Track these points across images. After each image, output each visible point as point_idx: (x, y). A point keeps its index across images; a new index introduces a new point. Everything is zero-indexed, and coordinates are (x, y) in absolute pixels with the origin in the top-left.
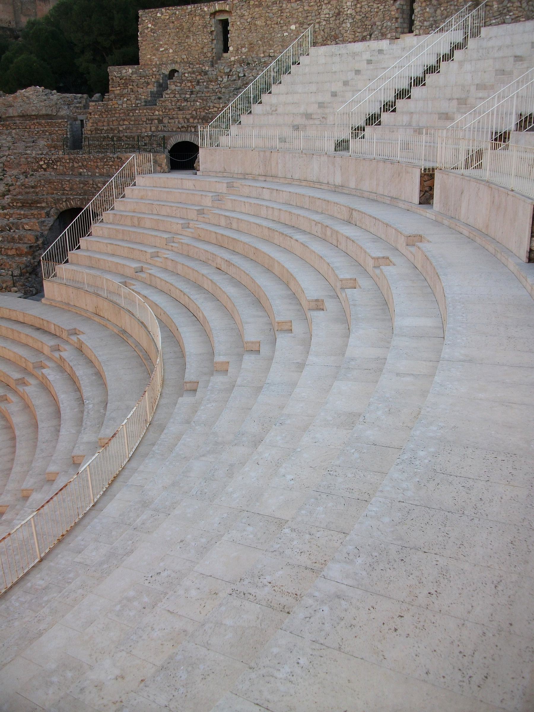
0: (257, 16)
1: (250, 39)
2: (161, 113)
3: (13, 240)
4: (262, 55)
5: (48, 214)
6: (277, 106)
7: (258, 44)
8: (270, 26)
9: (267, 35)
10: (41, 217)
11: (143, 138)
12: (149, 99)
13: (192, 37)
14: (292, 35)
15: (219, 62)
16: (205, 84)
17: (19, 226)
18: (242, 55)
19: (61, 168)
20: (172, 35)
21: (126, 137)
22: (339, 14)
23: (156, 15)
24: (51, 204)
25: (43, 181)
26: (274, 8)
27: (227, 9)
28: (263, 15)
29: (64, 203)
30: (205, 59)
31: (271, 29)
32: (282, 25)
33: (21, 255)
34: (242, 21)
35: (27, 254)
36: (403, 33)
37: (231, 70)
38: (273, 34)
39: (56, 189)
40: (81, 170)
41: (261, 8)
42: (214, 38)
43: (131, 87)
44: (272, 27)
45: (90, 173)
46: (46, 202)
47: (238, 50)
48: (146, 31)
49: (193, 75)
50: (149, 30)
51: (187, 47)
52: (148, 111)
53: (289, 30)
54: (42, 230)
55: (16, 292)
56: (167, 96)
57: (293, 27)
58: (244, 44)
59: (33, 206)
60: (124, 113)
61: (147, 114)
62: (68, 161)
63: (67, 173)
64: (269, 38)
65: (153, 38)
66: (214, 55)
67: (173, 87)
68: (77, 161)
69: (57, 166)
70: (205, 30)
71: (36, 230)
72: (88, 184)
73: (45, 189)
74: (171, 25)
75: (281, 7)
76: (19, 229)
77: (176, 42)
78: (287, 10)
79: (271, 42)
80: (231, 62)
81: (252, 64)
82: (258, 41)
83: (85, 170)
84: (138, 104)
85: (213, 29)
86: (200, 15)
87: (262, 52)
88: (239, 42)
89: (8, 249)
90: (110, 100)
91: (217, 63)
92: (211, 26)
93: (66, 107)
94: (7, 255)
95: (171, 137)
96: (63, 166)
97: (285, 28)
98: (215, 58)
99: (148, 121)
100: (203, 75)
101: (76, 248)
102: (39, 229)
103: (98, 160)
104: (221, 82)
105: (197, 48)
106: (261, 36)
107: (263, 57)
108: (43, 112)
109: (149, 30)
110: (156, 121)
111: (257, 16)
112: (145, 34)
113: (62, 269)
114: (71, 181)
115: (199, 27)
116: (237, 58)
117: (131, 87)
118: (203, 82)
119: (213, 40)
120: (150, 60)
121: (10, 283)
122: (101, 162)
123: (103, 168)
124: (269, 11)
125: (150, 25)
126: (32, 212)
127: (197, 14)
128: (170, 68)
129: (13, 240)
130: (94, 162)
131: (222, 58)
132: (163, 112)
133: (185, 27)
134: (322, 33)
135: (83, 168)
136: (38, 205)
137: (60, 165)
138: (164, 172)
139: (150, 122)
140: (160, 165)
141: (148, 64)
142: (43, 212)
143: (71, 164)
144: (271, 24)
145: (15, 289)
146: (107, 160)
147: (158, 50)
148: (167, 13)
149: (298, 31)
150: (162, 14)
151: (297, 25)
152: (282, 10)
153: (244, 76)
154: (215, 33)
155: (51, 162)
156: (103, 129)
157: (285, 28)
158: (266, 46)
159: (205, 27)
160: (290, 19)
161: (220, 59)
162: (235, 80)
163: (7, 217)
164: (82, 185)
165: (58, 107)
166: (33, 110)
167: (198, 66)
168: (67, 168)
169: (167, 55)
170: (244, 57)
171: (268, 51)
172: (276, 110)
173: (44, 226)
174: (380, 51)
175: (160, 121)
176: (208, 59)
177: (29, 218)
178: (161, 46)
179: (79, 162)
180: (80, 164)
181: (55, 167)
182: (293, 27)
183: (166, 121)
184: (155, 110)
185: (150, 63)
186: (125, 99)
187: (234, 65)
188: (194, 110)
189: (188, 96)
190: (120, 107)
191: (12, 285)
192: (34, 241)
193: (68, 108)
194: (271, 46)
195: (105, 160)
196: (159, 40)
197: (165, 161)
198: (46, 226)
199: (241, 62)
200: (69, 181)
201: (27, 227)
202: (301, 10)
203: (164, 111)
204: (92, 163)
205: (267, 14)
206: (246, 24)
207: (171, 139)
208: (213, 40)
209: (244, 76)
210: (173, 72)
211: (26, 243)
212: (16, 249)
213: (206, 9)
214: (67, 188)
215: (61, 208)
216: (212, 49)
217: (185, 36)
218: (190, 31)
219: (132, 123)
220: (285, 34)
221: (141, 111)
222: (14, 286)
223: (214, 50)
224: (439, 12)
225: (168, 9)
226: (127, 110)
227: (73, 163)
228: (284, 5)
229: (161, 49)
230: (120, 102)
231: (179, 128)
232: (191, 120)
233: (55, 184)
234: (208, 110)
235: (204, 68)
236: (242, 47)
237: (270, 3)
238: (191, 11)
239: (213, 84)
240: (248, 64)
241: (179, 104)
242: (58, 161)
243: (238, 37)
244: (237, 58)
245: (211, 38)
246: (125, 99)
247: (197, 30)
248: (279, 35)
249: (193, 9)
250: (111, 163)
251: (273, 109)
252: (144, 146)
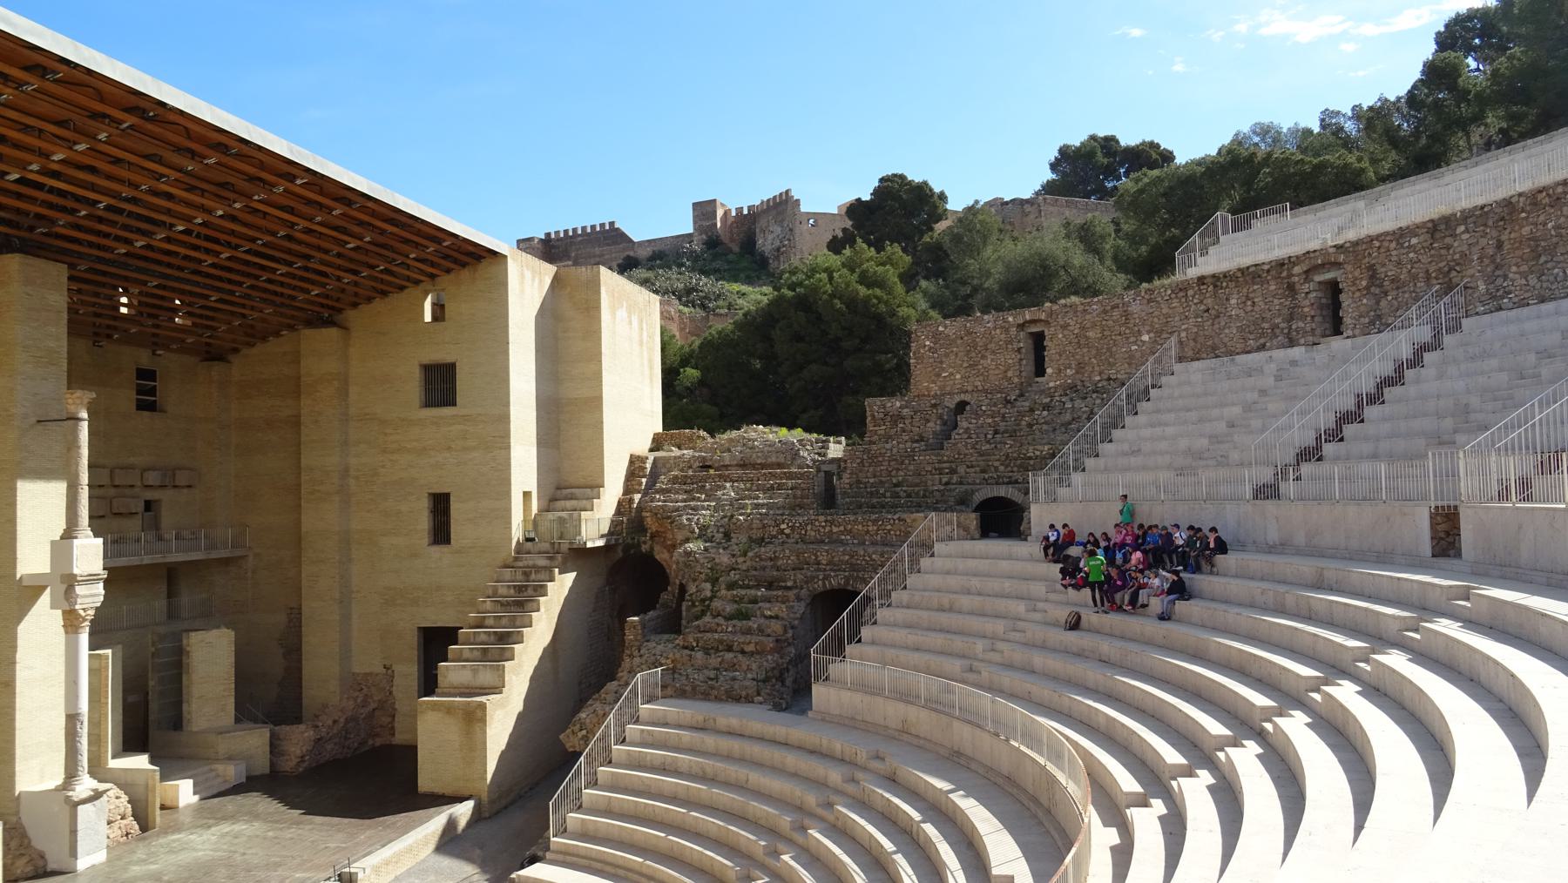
3: (748, 631)
35: (772, 651)
36: (1324, 336)
57: (1146, 338)
67: (965, 424)
90: (871, 443)
94: (743, 652)
113: (835, 669)
128: (957, 399)
129: (748, 631)
134: (1192, 344)
138: (973, 539)
142: (791, 594)
147: (938, 375)
159: (1011, 342)
174: (1294, 363)
178: (944, 370)
183: (962, 469)
224: (1383, 303)
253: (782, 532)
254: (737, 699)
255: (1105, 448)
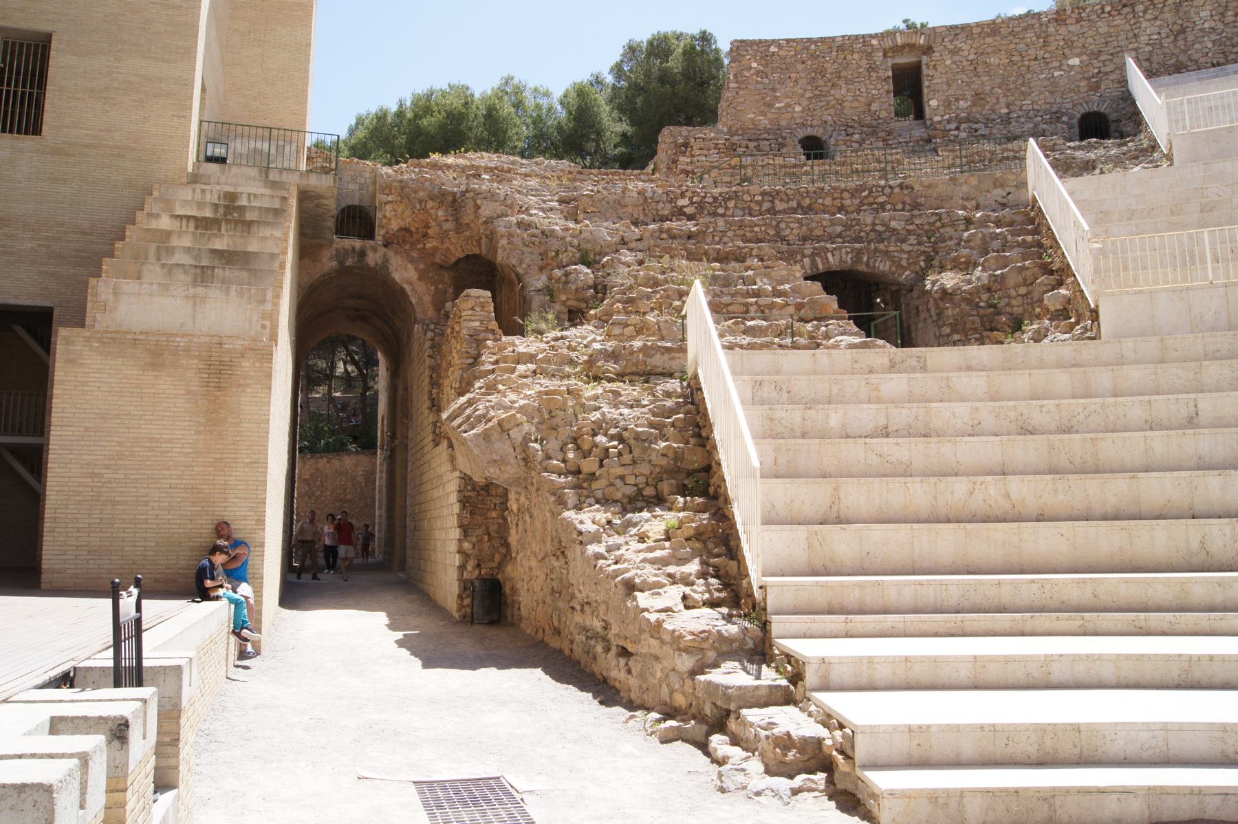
20: (800, 82)
22: (1183, 30)
28: (1003, 48)
34: (957, 58)
47: (949, 104)
50: (753, 71)
74: (800, 67)
77: (809, 94)
105: (855, 104)
109: (753, 71)
125: (754, 65)
137: (736, 207)
147: (770, 106)
169: (789, 115)
178: (777, 99)
180: (794, 204)
229: (777, 105)
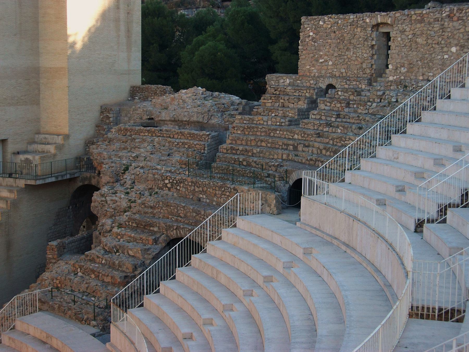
0: (419, 33)
1: (409, 58)
2: (300, 137)
4: (421, 78)
5: (156, 241)
6: (398, 154)
7: (418, 65)
8: (430, 46)
9: (427, 56)
10: (148, 243)
11: (270, 167)
12: (296, 117)
13: (352, 49)
14: (452, 58)
15: (379, 79)
16: (355, 106)
17: (125, 250)
18: (401, 75)
19: (184, 190)
20: (333, 46)
21: (255, 162)
23: (319, 23)
24: (163, 229)
25: (161, 203)
26: (435, 26)
27: (389, 22)
28: (425, 32)
29: (175, 231)
30: (364, 75)
31: (432, 49)
32: (443, 46)
33: (115, 284)
34: (403, 37)
37: (384, 93)
38: (433, 55)
39: (172, 214)
40: (201, 196)
41: (423, 25)
42: (374, 53)
43: (282, 101)
44: (432, 47)
45: (208, 201)
46: (159, 227)
47: (397, 69)
48: (307, 40)
49: (346, 94)
50: (310, 38)
51: (346, 60)
52: (288, 134)
53: (449, 53)
54: (144, 258)
55: (94, 326)
56: (313, 117)
57: (454, 49)
58: (404, 64)
59: (147, 229)
60: (265, 132)
61: (287, 136)
62: (190, 184)
63: (188, 197)
64: (429, 59)
65: (313, 48)
66: (373, 72)
67: (322, 106)
68: (198, 185)
69: (180, 187)
70: (366, 43)
71: (138, 258)
72: (200, 214)
73: (162, 211)
74: (333, 35)
75: (443, 25)
76: (124, 254)
77: (336, 54)
78: (449, 30)
79: (430, 64)
80: (389, 81)
81: (409, 87)
82: (417, 61)
83: (205, 197)
84: (282, 123)
85: (374, 43)
86: (361, 27)
87: (421, 74)
88: (398, 61)
89: (104, 275)
91: (376, 82)
92: (373, 40)
93: (219, 115)
94: (103, 281)
95: (294, 171)
96: (185, 188)
97: (445, 49)
98: (374, 75)
99: (283, 146)
100: (355, 95)
101: (155, 291)
102: (141, 257)
103: (217, 188)
104: (370, 106)
106: (420, 56)
107: (422, 80)
108: (195, 119)
109: (310, 38)
110: (291, 147)
111: (419, 33)
112: (306, 43)
114: (186, 208)
115: (360, 40)
116: (395, 78)
117: (282, 101)
118: (353, 104)
119: (373, 55)
120: (309, 71)
121: (91, 316)
122: (219, 190)
123: (221, 198)
124: (430, 28)
126: (141, 236)
127: (359, 26)
130: (213, 190)
131: (384, 75)
132: (302, 137)
133: (346, 38)
135: (203, 193)
136: (151, 229)
137: (183, 187)
138: (273, 214)
139: (286, 147)
140: (269, 206)
141: (306, 76)
143: (193, 188)
144: (432, 44)
145: (94, 323)
146: (225, 189)
147: (317, 61)
148: (330, 21)
149: (457, 55)
150: (324, 22)
151: (458, 48)
152: (443, 28)
153: (397, 101)
154: (376, 47)
155: (175, 182)
156: (238, 149)
157: (445, 49)
158: (425, 68)
159: (366, 40)
160: (451, 40)
161: (381, 76)
162: (385, 106)
163: (119, 237)
164: (194, 214)
165: (210, 114)
166: (185, 116)
167: (354, 83)
168: (189, 191)
169: (326, 67)
170: (402, 78)
171: (426, 73)
172: (398, 158)
173: (147, 254)
175: (295, 148)
176: (366, 75)
177: (137, 243)
178: (321, 57)
179: (200, 187)
180: (201, 189)
181: (178, 188)
182: (454, 49)
183: (300, 148)
184: (294, 133)
185: (308, 74)
186: (273, 115)
187: (391, 86)
188: (331, 139)
189: (333, 119)
190: (265, 123)
191: (93, 318)
192: (131, 270)
193: (222, 115)
194: (430, 68)
195: (223, 189)
196: (320, 50)
197: (274, 201)
198: (150, 254)
199: (399, 83)
200: (184, 207)
201: (131, 253)
202: (462, 30)
203: (303, 135)
204: (211, 190)
205: (429, 32)
206: (407, 41)
207: (294, 173)
208: (373, 55)
209: (397, 101)
210: (331, 86)
211: (124, 271)
212: (112, 277)
213: (368, 20)
214: (181, 214)
215: (172, 236)
216: (372, 65)
217: (346, 48)
218: (350, 43)
219: (269, 145)
220: (446, 57)
221: (281, 133)
222: (95, 320)
223: (374, 67)
225: (331, 18)
226: (269, 130)
227: (194, 186)
228: (446, 23)
229: (321, 61)
230: (265, 118)
231: (307, 160)
232: (324, 152)
233: (172, 208)
234: (344, 141)
235: (360, 86)
236: (402, 66)
237: (432, 20)
238: (353, 21)
239: (362, 108)
240: (406, 87)
241: (321, 128)
242: (181, 182)
243: (398, 55)
244: (395, 78)
245: (371, 52)
246: (273, 115)
247: (358, 43)
248: (439, 57)
249: (355, 19)
250: (228, 194)
251: (395, 156)
252: (267, 177)
253: (166, 185)
254: (81, 320)
255: (382, 152)
